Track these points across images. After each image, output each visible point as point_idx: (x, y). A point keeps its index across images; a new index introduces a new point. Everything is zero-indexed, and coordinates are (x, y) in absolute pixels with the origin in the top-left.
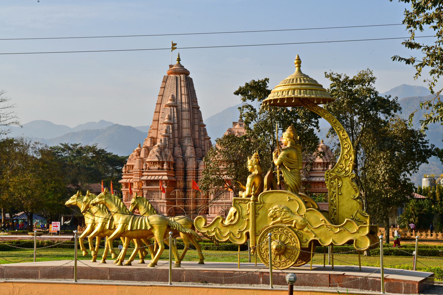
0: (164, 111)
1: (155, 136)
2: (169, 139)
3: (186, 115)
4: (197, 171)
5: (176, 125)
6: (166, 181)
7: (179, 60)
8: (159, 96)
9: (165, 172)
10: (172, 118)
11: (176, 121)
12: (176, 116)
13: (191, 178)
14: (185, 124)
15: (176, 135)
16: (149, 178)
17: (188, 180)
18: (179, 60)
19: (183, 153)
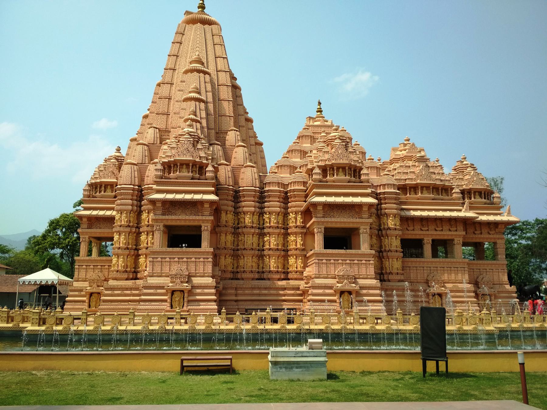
0: (184, 79)
1: (163, 126)
2: (202, 128)
3: (226, 93)
4: (262, 193)
5: (211, 106)
6: (212, 202)
7: (202, 7)
8: (169, 56)
9: (207, 185)
10: (203, 91)
11: (210, 99)
12: (209, 88)
13: (248, 205)
14: (228, 108)
15: (212, 125)
16: (170, 196)
17: (245, 209)
18: (202, 7)
19: (228, 158)
